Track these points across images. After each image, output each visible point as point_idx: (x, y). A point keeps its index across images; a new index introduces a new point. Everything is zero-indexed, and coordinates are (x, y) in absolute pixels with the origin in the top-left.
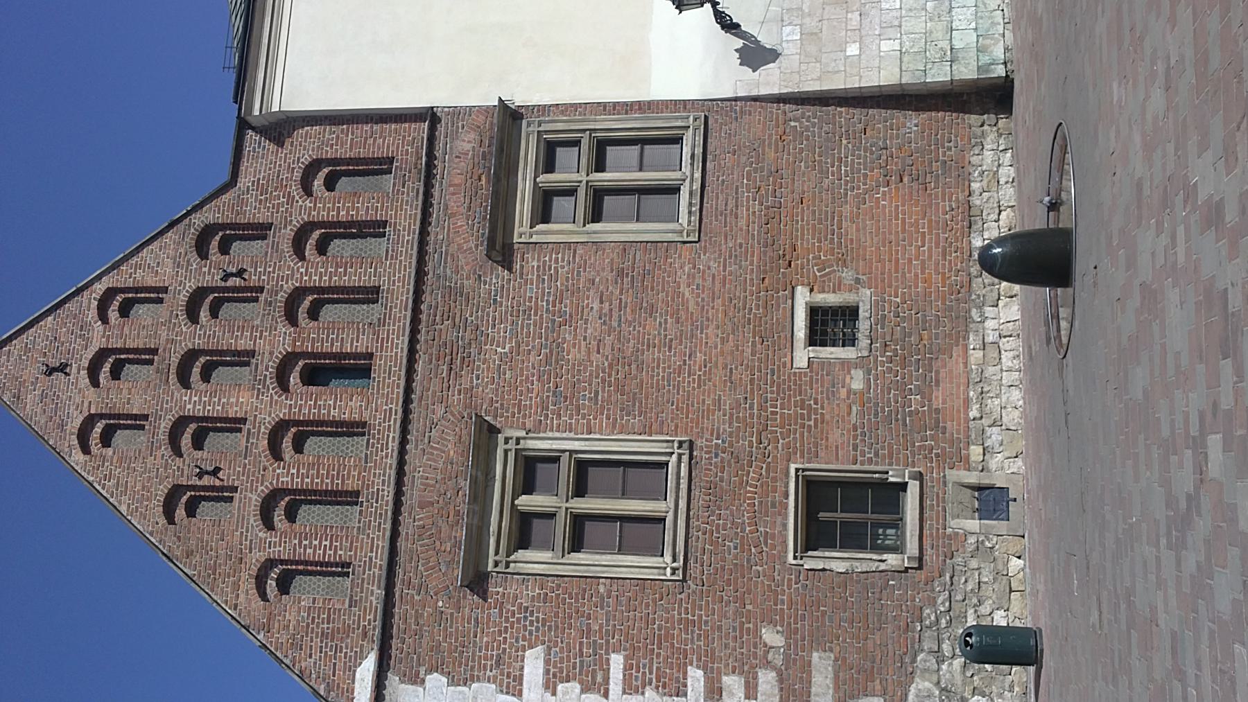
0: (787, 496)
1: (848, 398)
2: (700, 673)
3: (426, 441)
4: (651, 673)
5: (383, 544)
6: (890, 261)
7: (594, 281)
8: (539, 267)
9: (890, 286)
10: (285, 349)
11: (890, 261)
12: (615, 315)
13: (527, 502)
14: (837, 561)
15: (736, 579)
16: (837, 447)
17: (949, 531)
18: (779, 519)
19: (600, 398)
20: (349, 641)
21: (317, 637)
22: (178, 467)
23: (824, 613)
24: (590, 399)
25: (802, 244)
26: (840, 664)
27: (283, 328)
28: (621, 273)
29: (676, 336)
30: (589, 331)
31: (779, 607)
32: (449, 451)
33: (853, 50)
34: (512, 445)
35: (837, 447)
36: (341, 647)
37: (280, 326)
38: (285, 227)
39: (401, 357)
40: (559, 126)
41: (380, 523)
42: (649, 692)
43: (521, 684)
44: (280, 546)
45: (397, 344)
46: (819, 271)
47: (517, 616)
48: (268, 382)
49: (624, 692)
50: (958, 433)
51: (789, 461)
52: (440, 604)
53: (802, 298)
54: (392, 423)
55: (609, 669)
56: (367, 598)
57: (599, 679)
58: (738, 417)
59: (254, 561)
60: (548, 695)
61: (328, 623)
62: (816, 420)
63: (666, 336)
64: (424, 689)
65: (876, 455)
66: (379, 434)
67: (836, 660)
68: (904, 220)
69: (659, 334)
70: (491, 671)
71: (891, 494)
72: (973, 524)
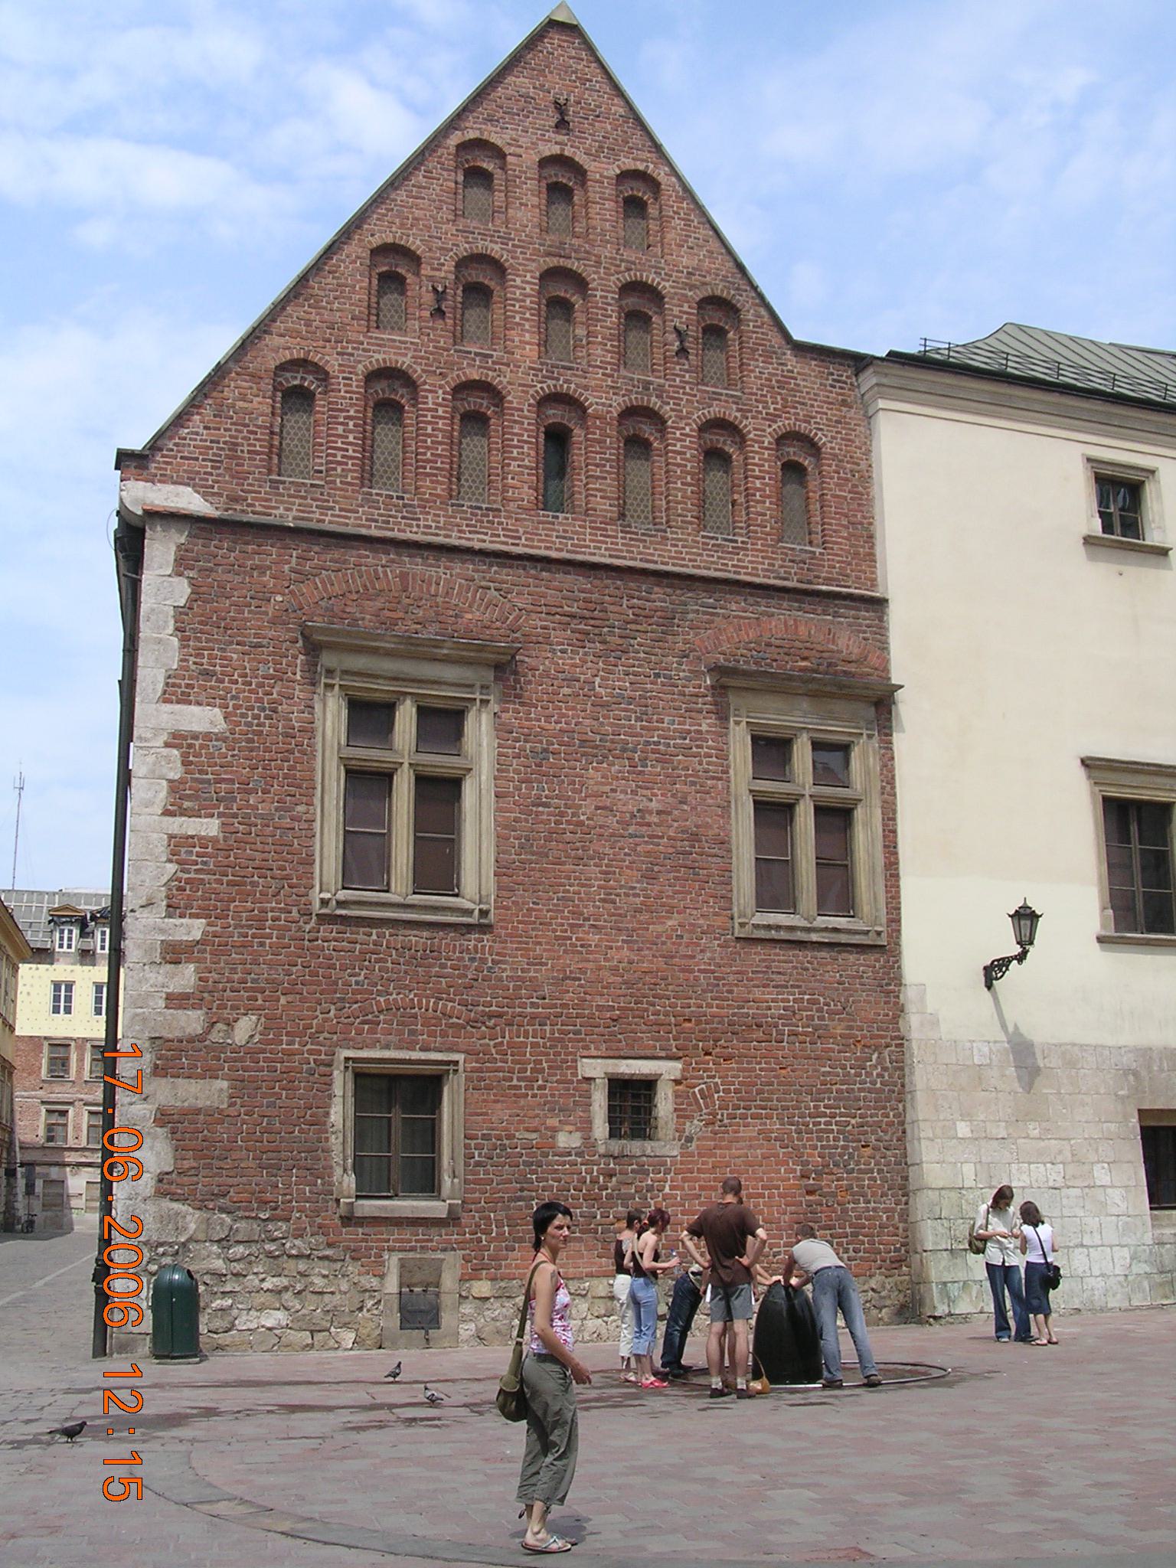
10: (591, 405)
20: (227, 478)
21: (230, 436)
27: (618, 403)
36: (219, 468)
37: (621, 400)
38: (739, 410)
41: (376, 521)
44: (346, 392)
48: (551, 382)
56: (282, 502)
59: (327, 358)
61: (249, 452)
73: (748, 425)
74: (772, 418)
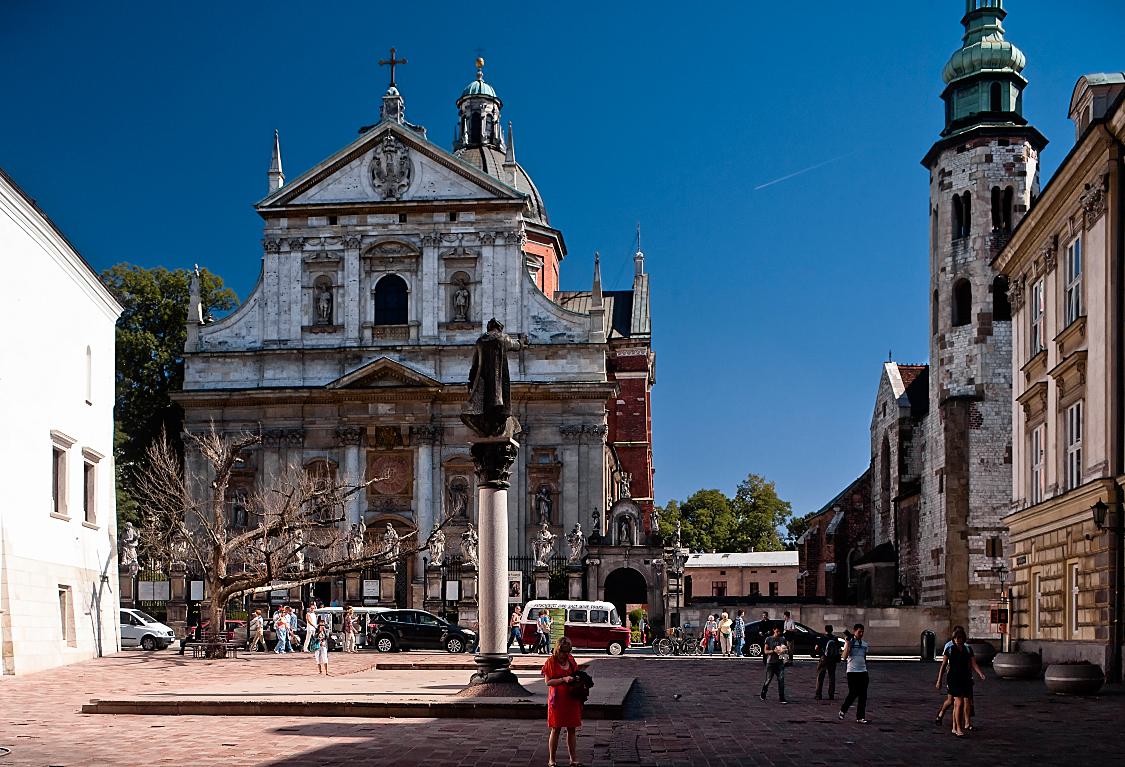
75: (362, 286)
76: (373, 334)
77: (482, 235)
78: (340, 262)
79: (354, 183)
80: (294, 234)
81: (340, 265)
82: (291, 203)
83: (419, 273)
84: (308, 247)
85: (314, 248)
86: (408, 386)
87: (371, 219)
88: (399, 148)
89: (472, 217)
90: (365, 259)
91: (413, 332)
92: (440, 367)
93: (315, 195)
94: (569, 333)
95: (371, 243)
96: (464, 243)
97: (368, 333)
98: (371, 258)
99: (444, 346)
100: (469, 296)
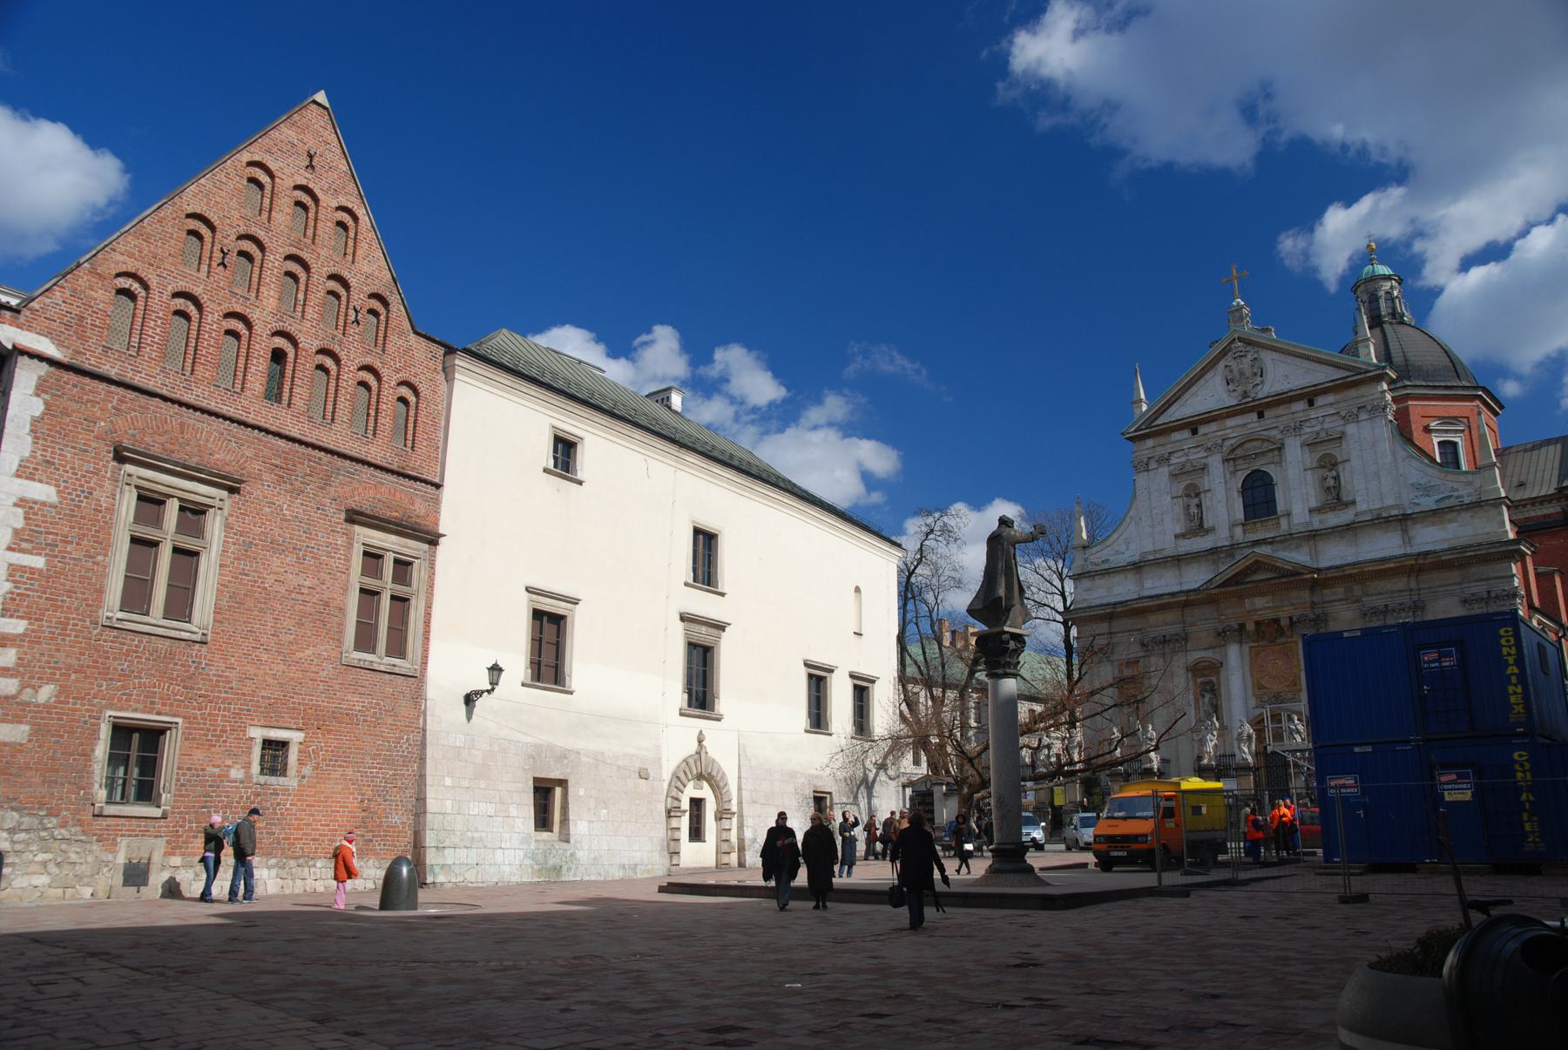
0: (158, 713)
1: (225, 766)
2: (20, 630)
3: (229, 438)
4: (26, 589)
5: (150, 385)
6: (315, 801)
7: (324, 584)
8: (336, 544)
9: (298, 800)
10: (301, 342)
11: (315, 801)
12: (300, 597)
13: (172, 508)
14: (101, 750)
15: (98, 668)
16: (190, 755)
17: (119, 839)
18: (141, 706)
19: (244, 577)
20: (74, 338)
21: (80, 312)
22: (229, 236)
23: (62, 736)
24: (244, 569)
25: (331, 738)
26: (17, 748)
27: (317, 344)
28: (326, 604)
29: (280, 640)
30: (291, 576)
31: (71, 700)
32: (219, 454)
33: (448, 781)
34: (217, 503)
35: (190, 755)
36: (70, 330)
37: (318, 343)
38: (381, 362)
39: (285, 429)
40: (418, 572)
41: (167, 386)
42: (8, 586)
43: (27, 478)
44: (159, 301)
45: (294, 428)
46: (313, 750)
47: (86, 485)
49: (10, 565)
50: (192, 848)
51: (184, 717)
52: (103, 424)
53: (294, 737)
54: (241, 412)
55: (32, 554)
56: (109, 362)
57: (25, 545)
58: (219, 681)
59: (150, 276)
60: (14, 500)
61: (91, 324)
62: (211, 741)
63: (281, 633)
64: (31, 395)
65: (182, 785)
66: (234, 400)
67: (21, 745)
68: (338, 812)
69: (284, 628)
70: (42, 455)
71: (146, 793)
72: (121, 859)
73: (384, 372)
74: (397, 371)
75: (1228, 486)
76: (1244, 530)
77: (1343, 413)
78: (1204, 468)
79: (1211, 394)
80: (1161, 451)
81: (1206, 471)
82: (1154, 424)
83: (1284, 464)
84: (1174, 460)
85: (1179, 460)
86: (1283, 576)
87: (1231, 422)
88: (1248, 352)
89: (1330, 398)
90: (1228, 460)
91: (1284, 522)
92: (1316, 552)
93: (1179, 412)
94: (1456, 494)
95: (1232, 445)
96: (1326, 426)
97: (1238, 531)
98: (1234, 459)
99: (1316, 531)
100: (1338, 475)
